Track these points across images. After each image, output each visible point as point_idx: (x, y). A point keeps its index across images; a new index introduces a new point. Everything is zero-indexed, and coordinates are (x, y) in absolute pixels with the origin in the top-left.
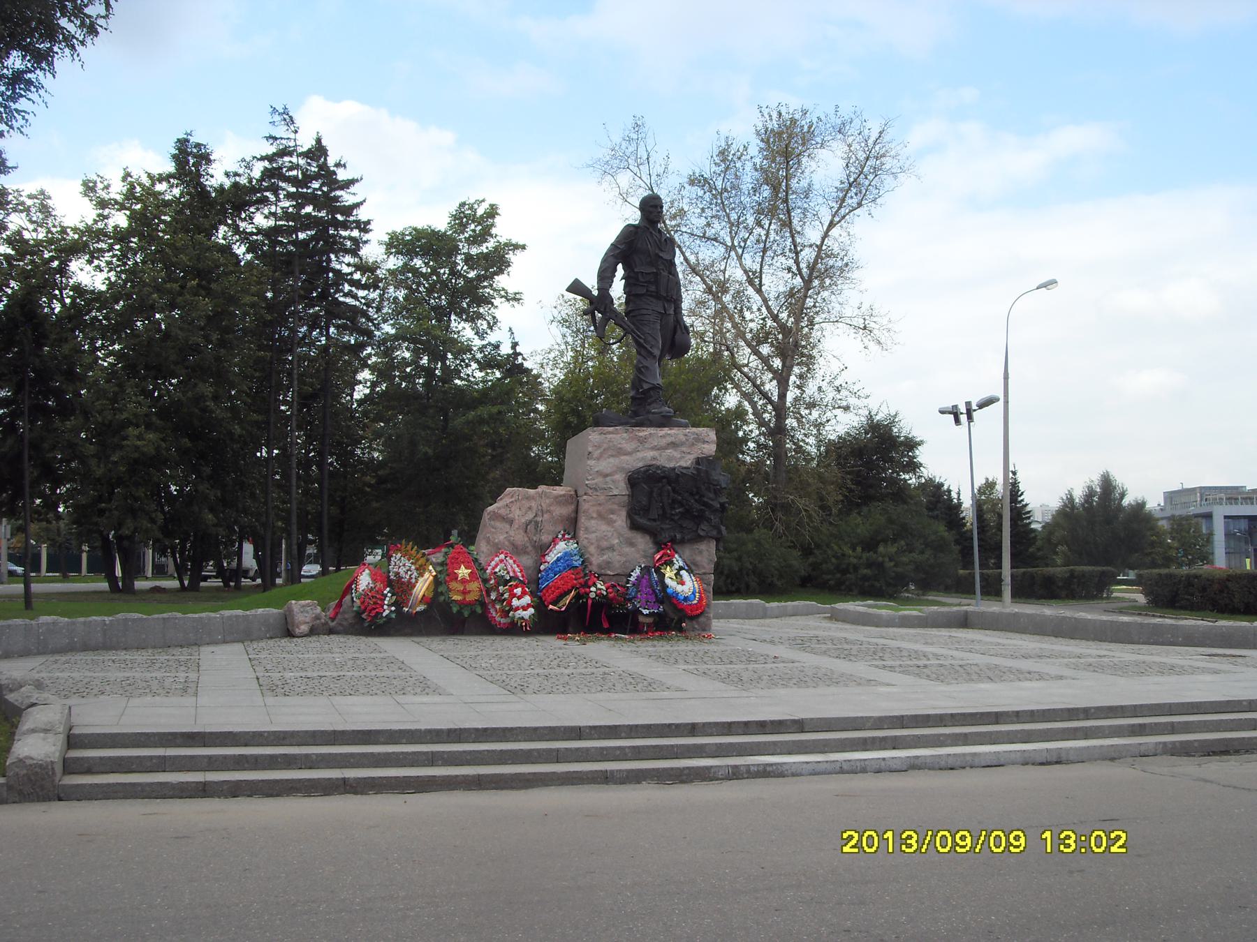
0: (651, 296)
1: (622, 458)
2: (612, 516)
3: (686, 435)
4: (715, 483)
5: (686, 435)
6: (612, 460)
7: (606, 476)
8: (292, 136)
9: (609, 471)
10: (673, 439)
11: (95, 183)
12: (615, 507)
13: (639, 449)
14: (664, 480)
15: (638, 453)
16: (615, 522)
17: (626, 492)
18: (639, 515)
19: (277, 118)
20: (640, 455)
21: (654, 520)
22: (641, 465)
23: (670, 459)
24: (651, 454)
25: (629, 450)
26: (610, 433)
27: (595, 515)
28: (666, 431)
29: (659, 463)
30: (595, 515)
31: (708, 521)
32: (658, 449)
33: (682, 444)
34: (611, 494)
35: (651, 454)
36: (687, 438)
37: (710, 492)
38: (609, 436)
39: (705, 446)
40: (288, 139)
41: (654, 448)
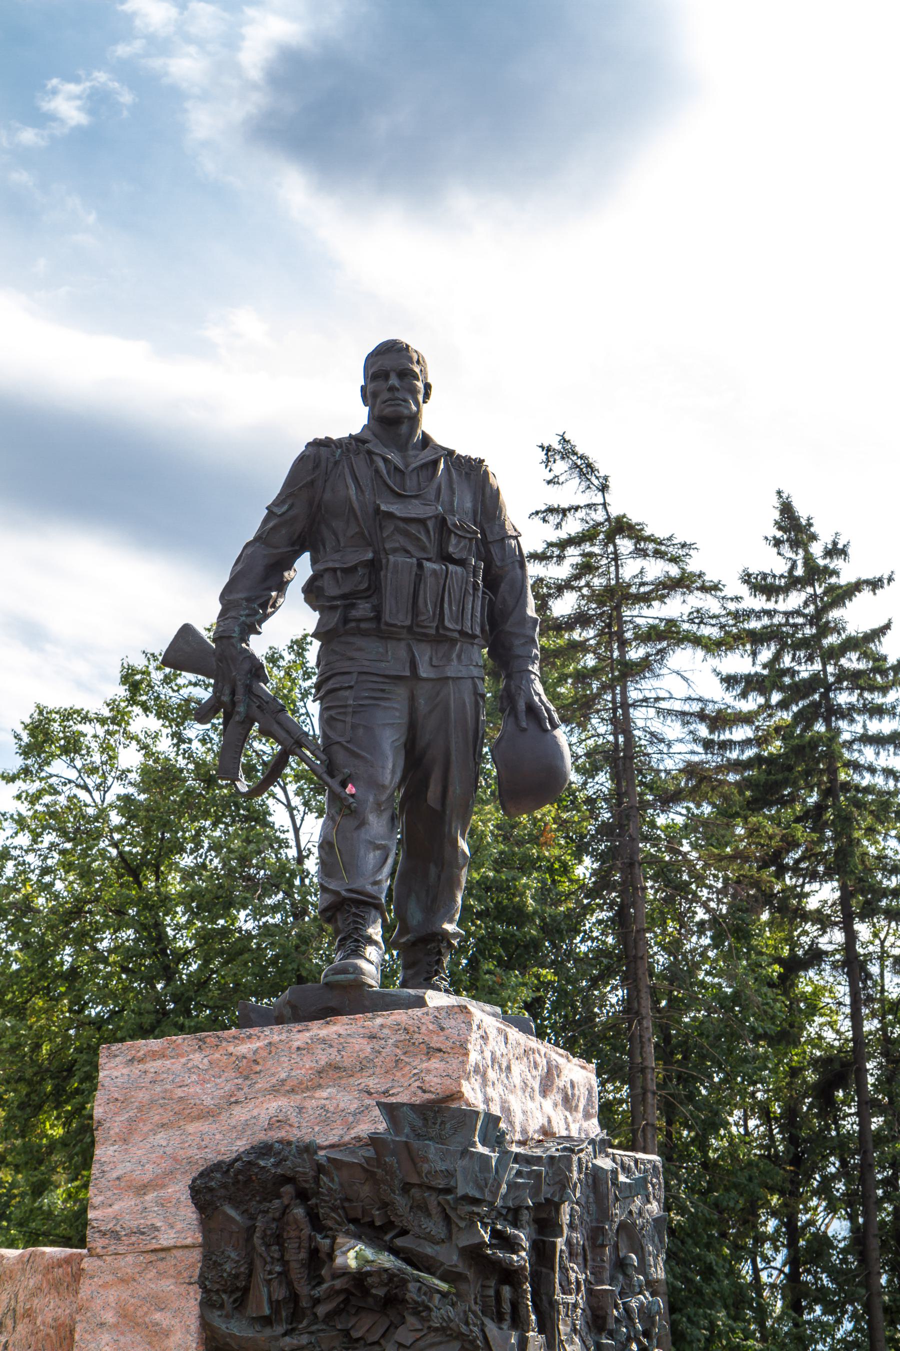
0: (364, 634)
1: (191, 1128)
2: (158, 1316)
3: (372, 1037)
4: (441, 1183)
5: (372, 1037)
6: (160, 1138)
7: (142, 1189)
8: (599, 499)
9: (149, 1172)
10: (333, 1055)
11: (146, 673)
12: (167, 1285)
13: (240, 1095)
14: (288, 1189)
15: (237, 1110)
16: (167, 1334)
17: (194, 1236)
18: (222, 1306)
19: (560, 467)
20: (240, 1114)
21: (266, 1321)
22: (241, 1145)
23: (326, 1117)
24: (274, 1106)
25: (208, 1101)
26: (155, 1055)
27: (109, 1317)
28: (318, 1029)
29: (294, 1135)
30: (109, 1317)
31: (416, 1313)
32: (293, 1091)
33: (363, 1066)
34: (154, 1245)
35: (274, 1106)
36: (376, 1044)
37: (429, 1215)
38: (153, 1066)
39: (435, 1063)
40: (589, 506)
41: (275, 1090)
